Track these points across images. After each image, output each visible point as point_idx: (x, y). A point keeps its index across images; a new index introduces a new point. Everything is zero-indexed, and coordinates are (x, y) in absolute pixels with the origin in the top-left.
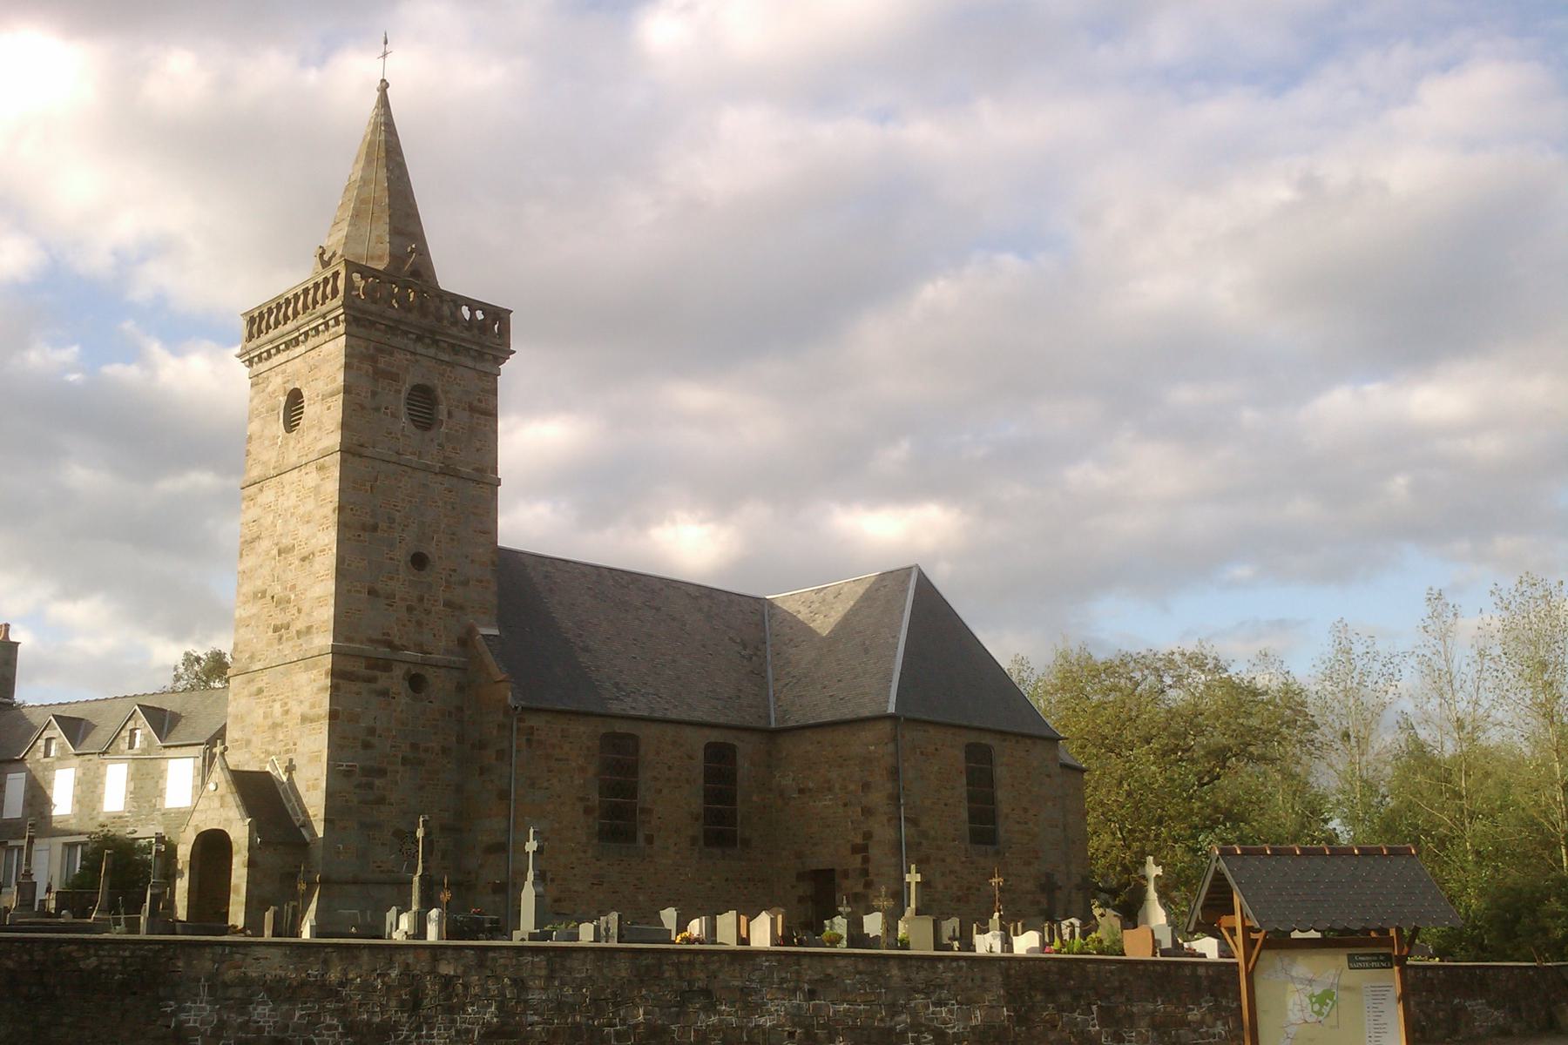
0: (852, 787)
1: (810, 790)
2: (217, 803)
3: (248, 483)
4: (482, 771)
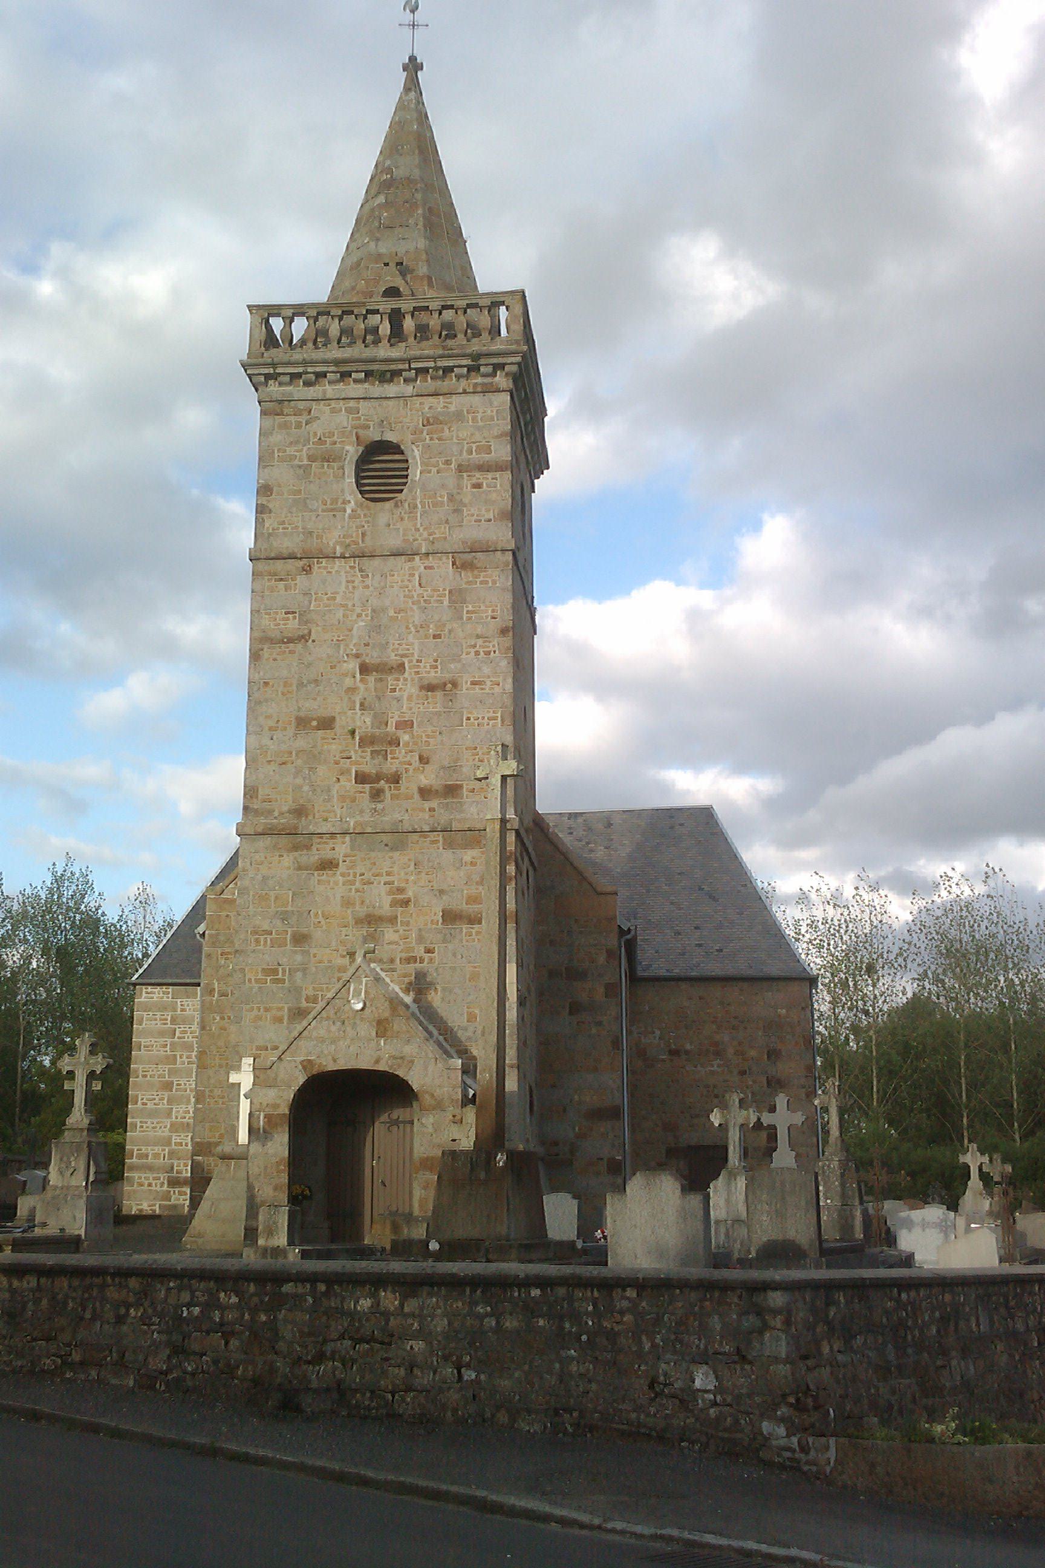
0: (753, 1053)
1: (687, 1052)
2: (366, 1030)
3: (273, 555)
4: (575, 1008)
